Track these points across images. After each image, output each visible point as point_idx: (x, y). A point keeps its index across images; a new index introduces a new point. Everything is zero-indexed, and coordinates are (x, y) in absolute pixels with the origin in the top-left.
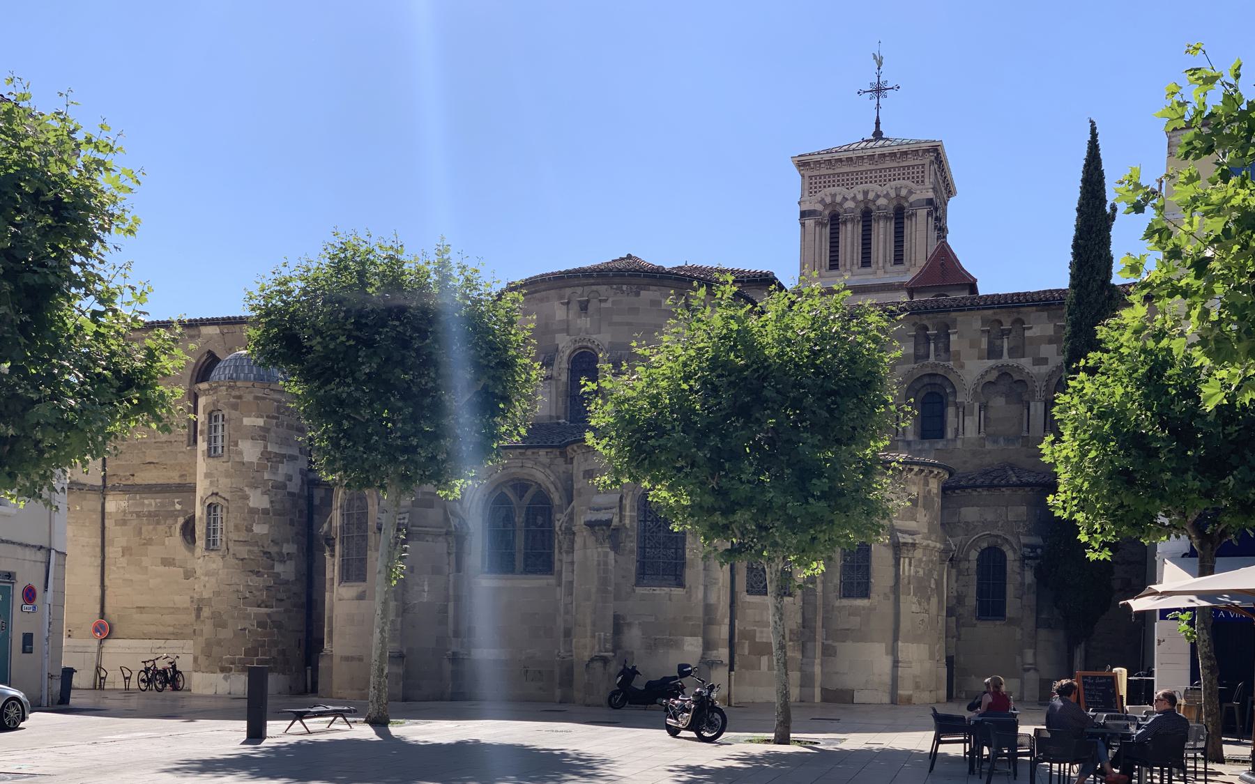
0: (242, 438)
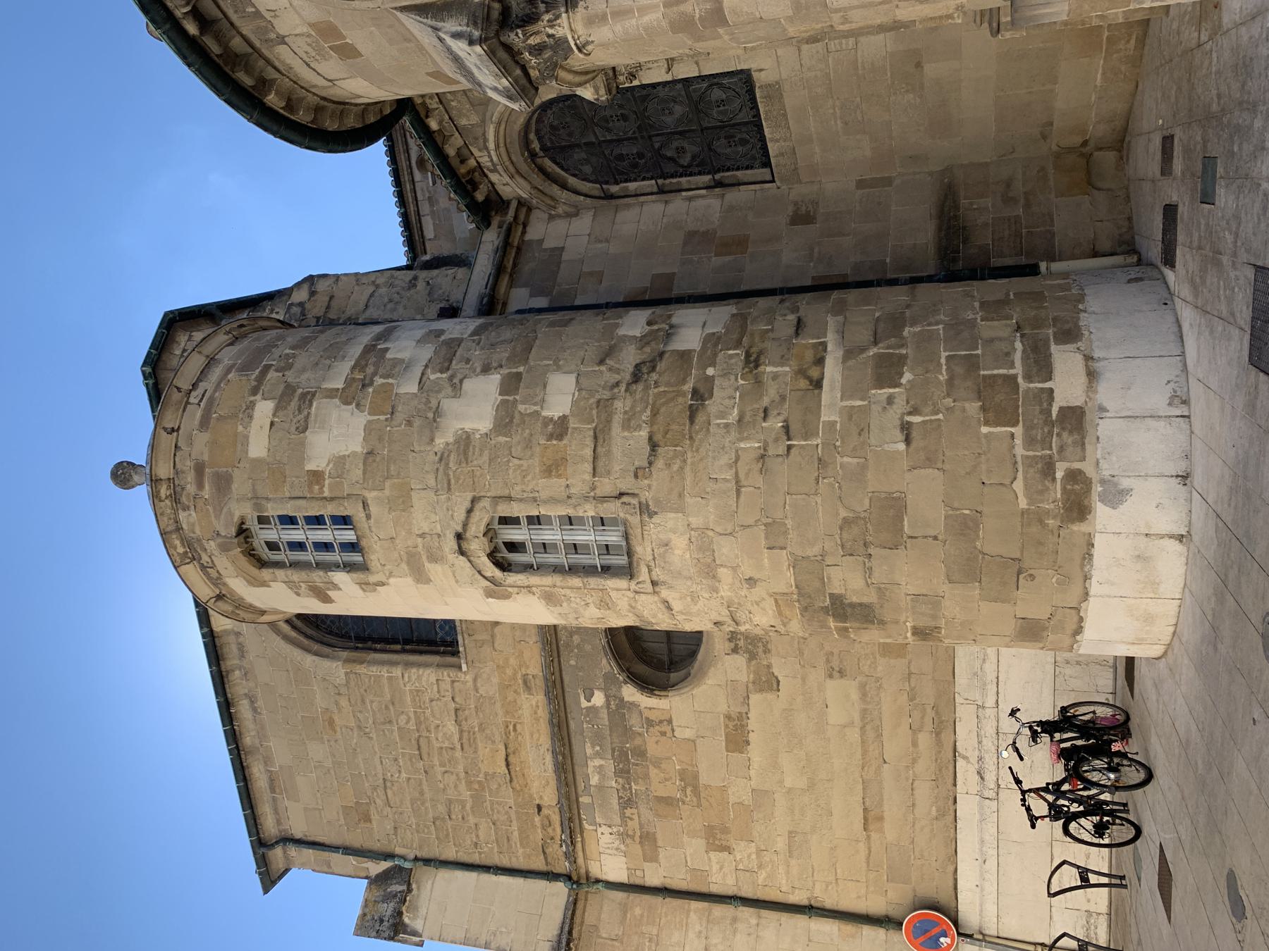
0: (301, 460)
